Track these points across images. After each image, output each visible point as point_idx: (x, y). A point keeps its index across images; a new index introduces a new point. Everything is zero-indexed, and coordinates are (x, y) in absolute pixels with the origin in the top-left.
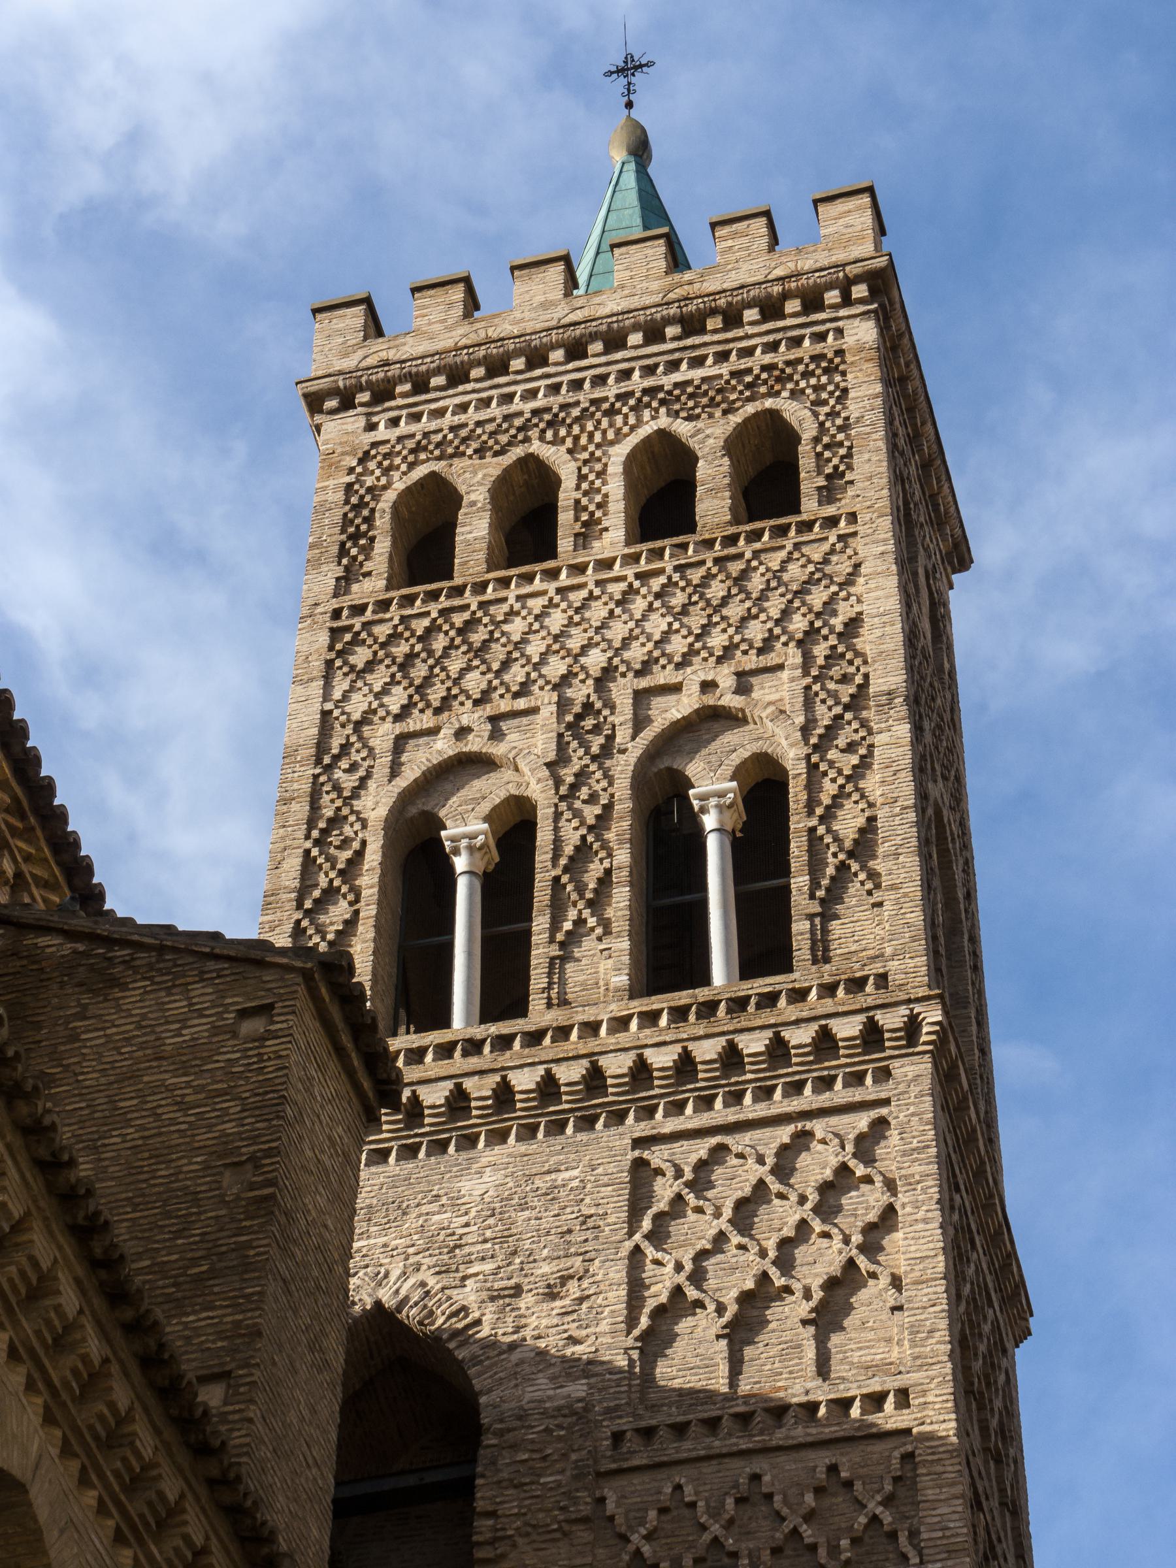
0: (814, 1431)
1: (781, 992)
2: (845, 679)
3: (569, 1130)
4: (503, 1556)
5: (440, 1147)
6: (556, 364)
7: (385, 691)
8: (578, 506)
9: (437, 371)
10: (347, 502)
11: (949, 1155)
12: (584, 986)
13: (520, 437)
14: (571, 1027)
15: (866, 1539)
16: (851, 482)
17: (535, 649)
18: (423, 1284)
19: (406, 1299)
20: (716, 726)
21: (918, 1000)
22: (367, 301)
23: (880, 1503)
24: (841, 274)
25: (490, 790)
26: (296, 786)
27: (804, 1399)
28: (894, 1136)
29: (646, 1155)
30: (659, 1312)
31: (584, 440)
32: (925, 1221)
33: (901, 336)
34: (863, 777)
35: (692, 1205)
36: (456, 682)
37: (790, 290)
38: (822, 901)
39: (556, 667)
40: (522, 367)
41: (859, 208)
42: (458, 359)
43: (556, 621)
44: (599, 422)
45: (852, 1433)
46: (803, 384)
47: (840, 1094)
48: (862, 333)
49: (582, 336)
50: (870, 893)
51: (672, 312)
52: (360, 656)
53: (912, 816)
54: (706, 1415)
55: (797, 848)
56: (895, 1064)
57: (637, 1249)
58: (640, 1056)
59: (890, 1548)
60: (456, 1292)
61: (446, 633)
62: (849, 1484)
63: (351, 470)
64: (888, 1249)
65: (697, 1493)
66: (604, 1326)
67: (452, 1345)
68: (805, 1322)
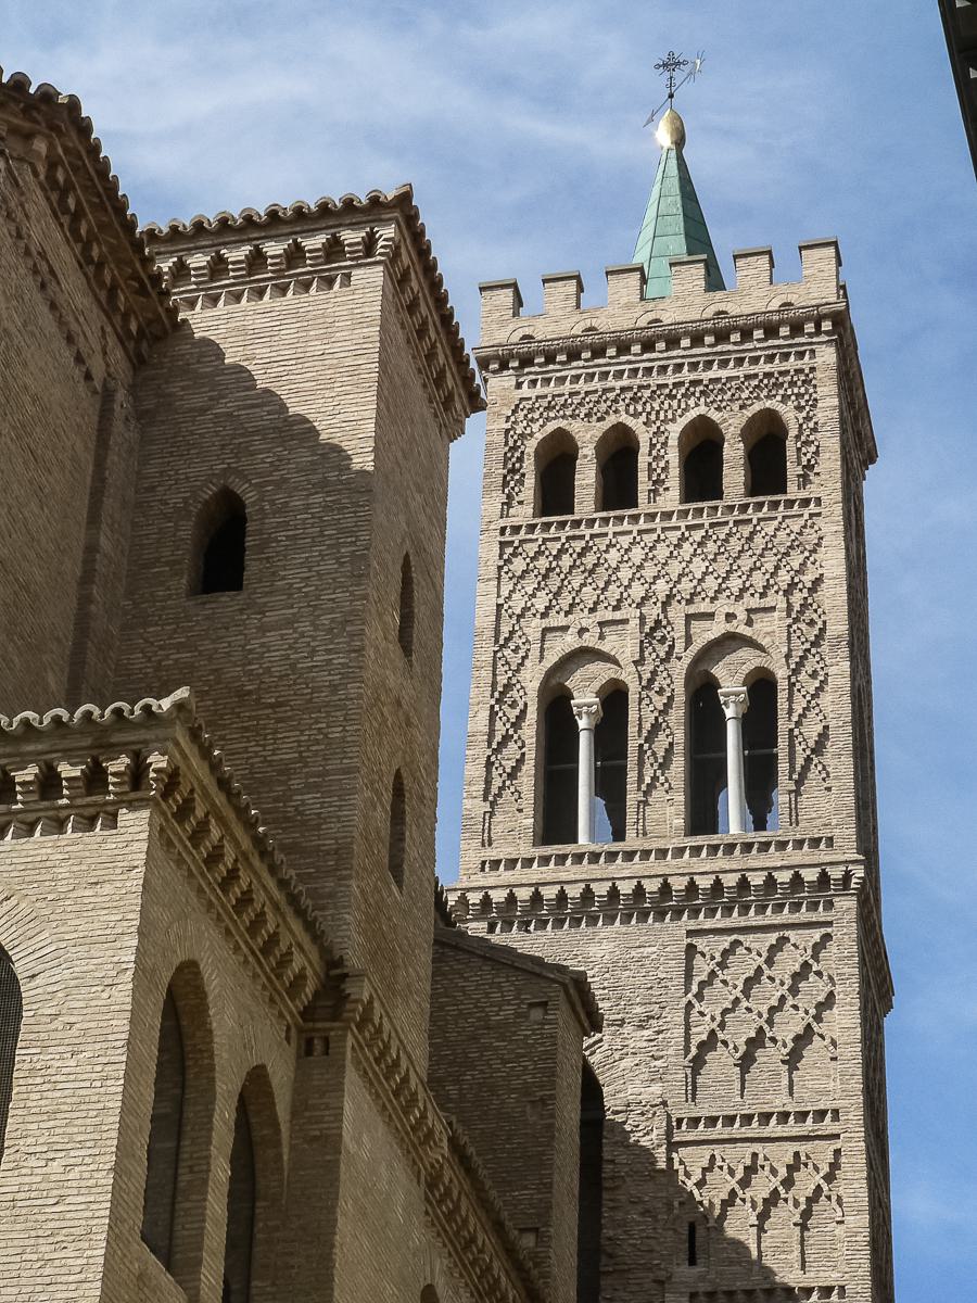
3: (650, 920)
5: (576, 922)
6: (635, 355)
7: (533, 595)
8: (651, 470)
10: (506, 444)
17: (625, 574)
20: (734, 644)
22: (514, 286)
27: (781, 1109)
29: (694, 941)
30: (701, 1045)
31: (653, 417)
32: (851, 1005)
33: (848, 346)
39: (638, 591)
40: (614, 354)
43: (637, 554)
44: (663, 403)
46: (789, 392)
48: (827, 356)
51: (709, 326)
52: (519, 565)
53: (850, 729)
55: (783, 743)
56: (837, 899)
57: (690, 1002)
61: (571, 555)
63: (508, 418)
67: (587, 1053)
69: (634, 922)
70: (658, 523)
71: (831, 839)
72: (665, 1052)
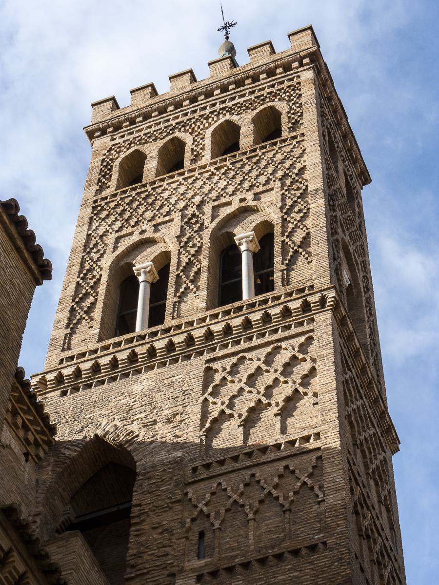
0: (278, 454)
1: (269, 299)
2: (298, 189)
4: (144, 521)
6: (186, 106)
7: (113, 224)
9: (139, 116)
11: (342, 349)
12: (188, 311)
13: (171, 132)
14: (182, 324)
15: (301, 492)
16: (302, 124)
18: (115, 425)
19: (108, 431)
20: (246, 214)
21: (325, 290)
23: (306, 477)
24: (298, 56)
25: (154, 251)
26: (75, 261)
27: (274, 443)
28: (315, 342)
29: (211, 365)
30: (215, 421)
33: (327, 80)
34: (305, 220)
35: (229, 380)
36: (141, 216)
37: (278, 64)
38: (287, 265)
39: (182, 204)
41: (306, 35)
42: (147, 110)
44: (202, 122)
45: (295, 452)
47: (294, 330)
48: (308, 75)
49: (196, 94)
50: (307, 259)
51: (231, 80)
52: (104, 214)
53: (325, 229)
54: (232, 455)
56: (317, 316)
57: (206, 399)
58: (208, 329)
59: (311, 494)
60: (129, 426)
62: (293, 472)
63: (105, 154)
64: (313, 384)
65: (227, 485)
66: (191, 429)
67: (126, 446)
68: (276, 415)
69: (167, 365)
70: (196, 173)
71: (312, 287)
72: (186, 431)
